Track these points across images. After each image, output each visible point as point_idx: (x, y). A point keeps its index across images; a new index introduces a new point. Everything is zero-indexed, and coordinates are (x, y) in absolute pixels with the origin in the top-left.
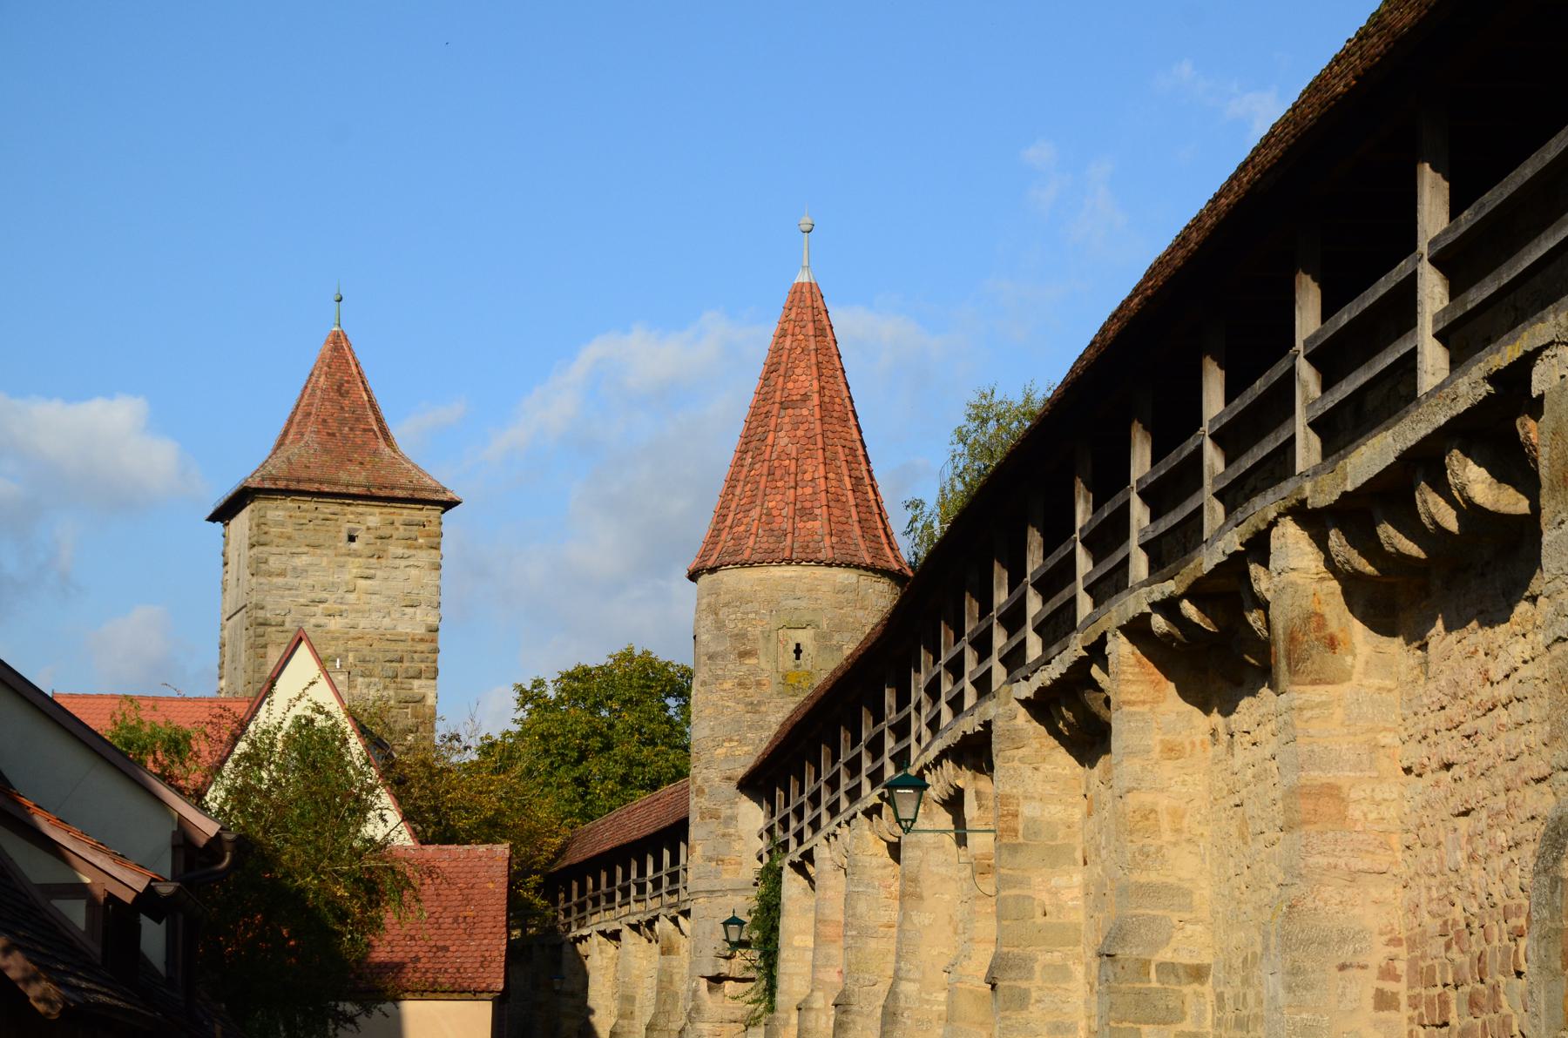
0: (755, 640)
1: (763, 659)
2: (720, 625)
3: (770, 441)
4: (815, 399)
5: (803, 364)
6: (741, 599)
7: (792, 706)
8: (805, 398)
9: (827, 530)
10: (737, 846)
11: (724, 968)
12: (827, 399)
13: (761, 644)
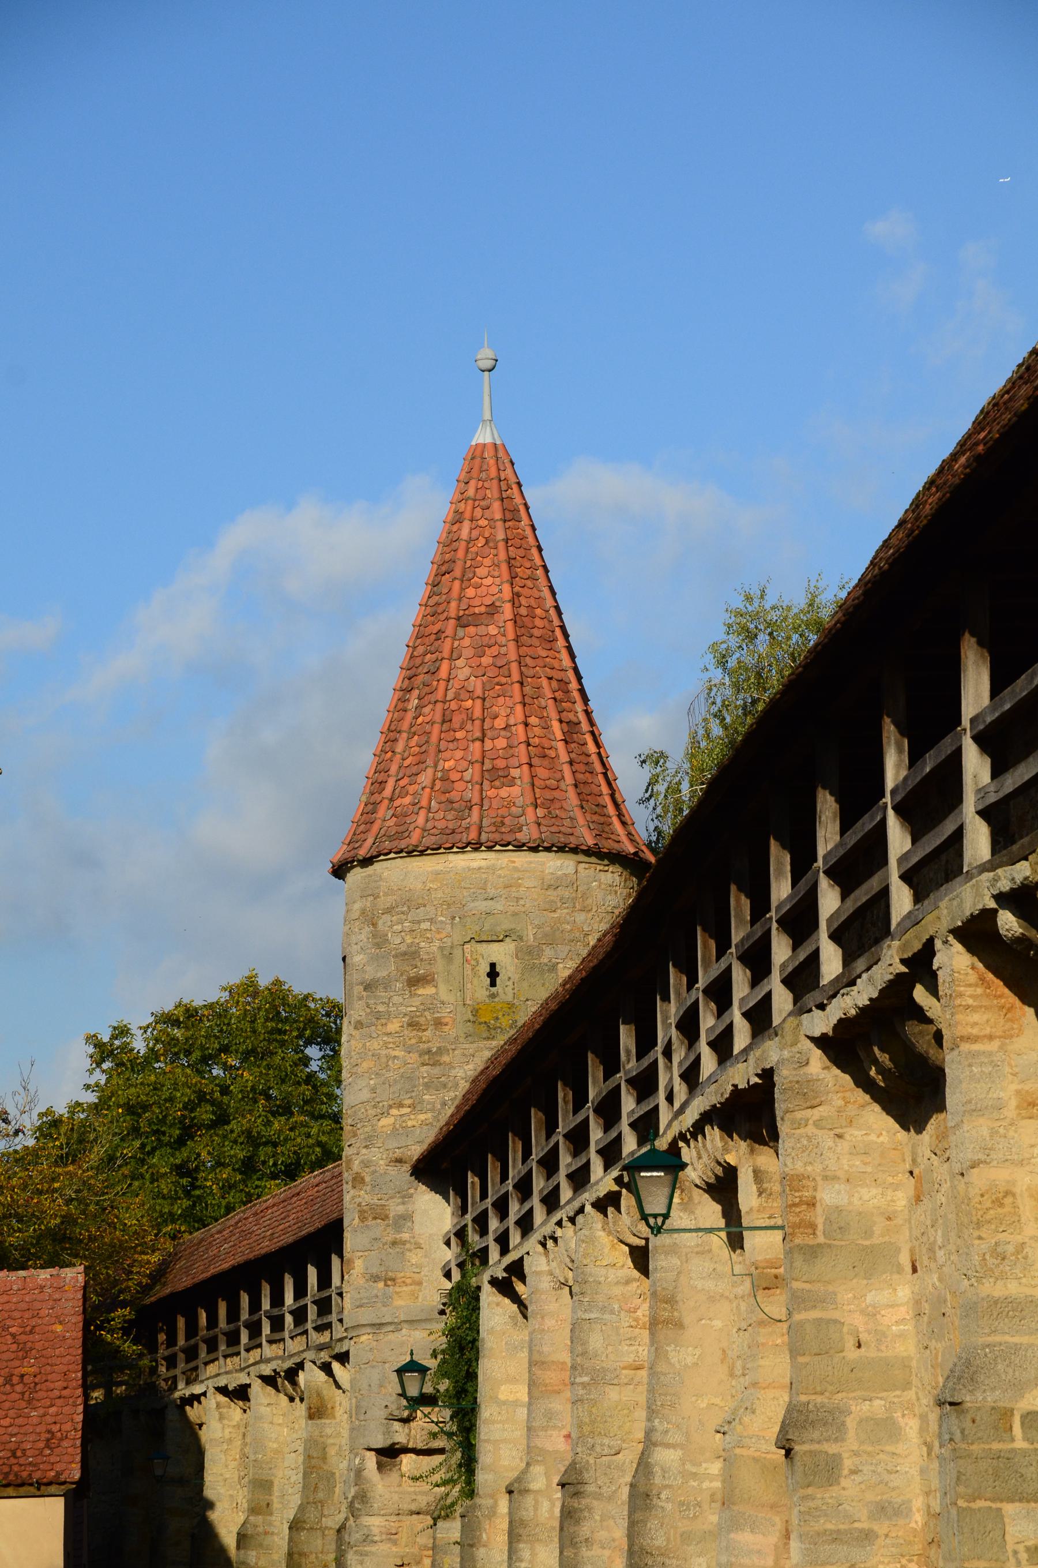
0: (431, 961)
1: (443, 988)
2: (380, 941)
3: (443, 673)
4: (507, 608)
5: (487, 562)
6: (409, 903)
7: (488, 1054)
8: (493, 610)
9: (529, 799)
10: (414, 1257)
11: (400, 1435)
12: (523, 611)
13: (440, 966)
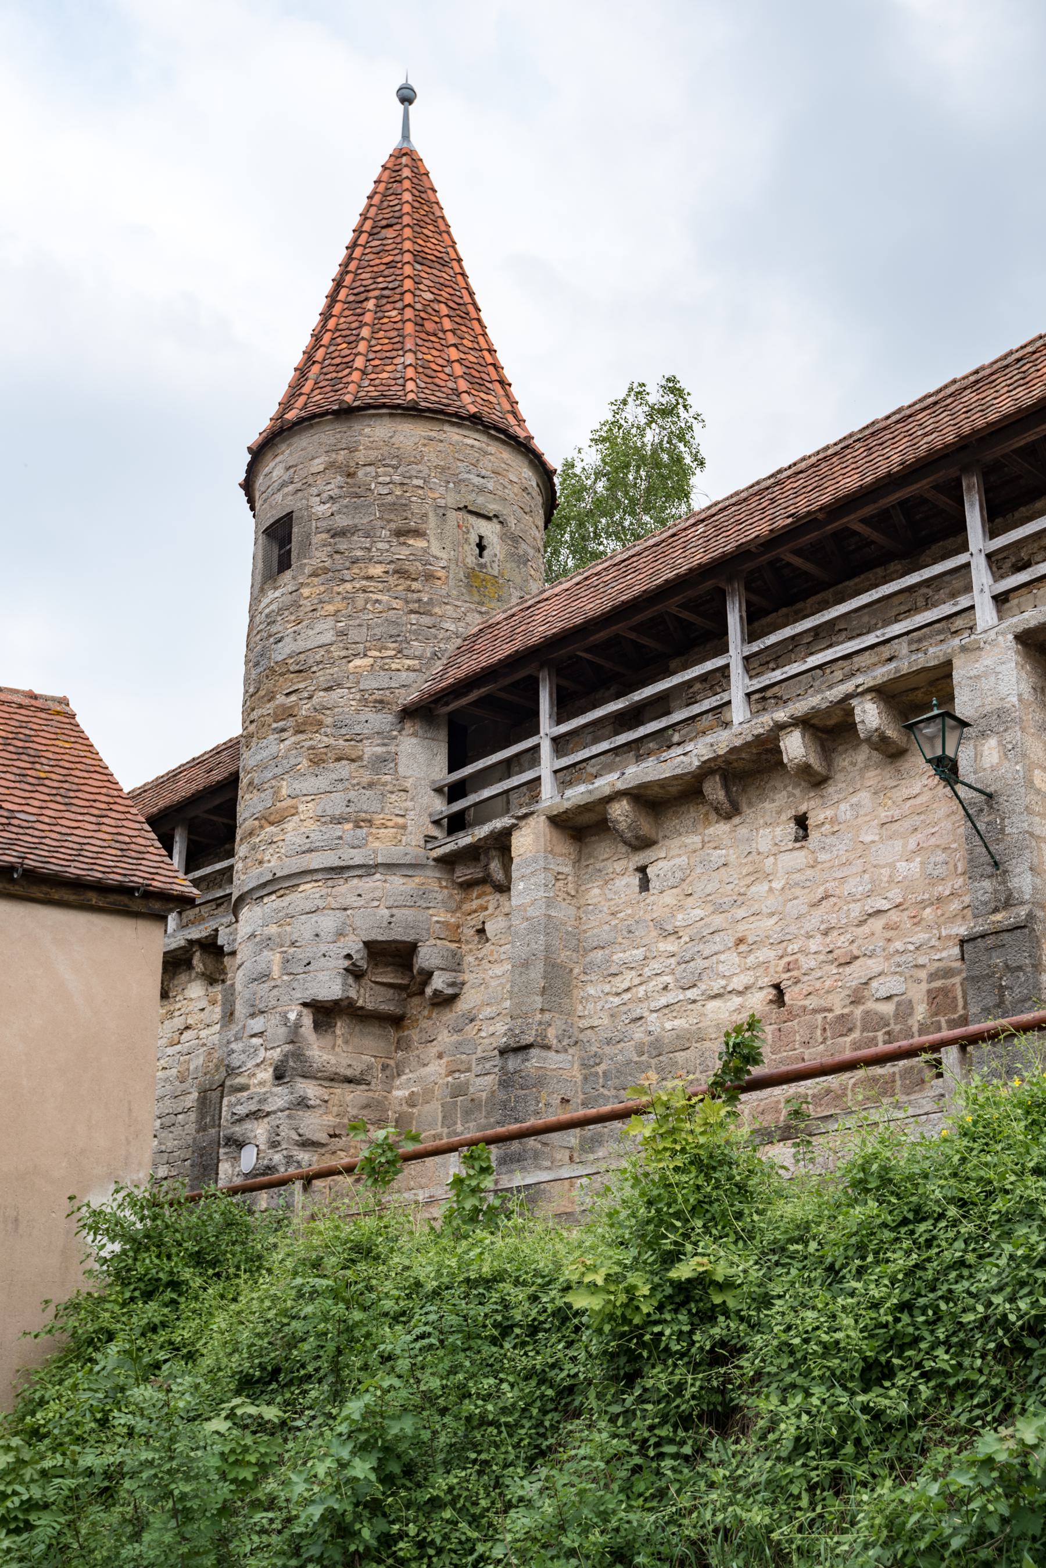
13: (432, 521)
